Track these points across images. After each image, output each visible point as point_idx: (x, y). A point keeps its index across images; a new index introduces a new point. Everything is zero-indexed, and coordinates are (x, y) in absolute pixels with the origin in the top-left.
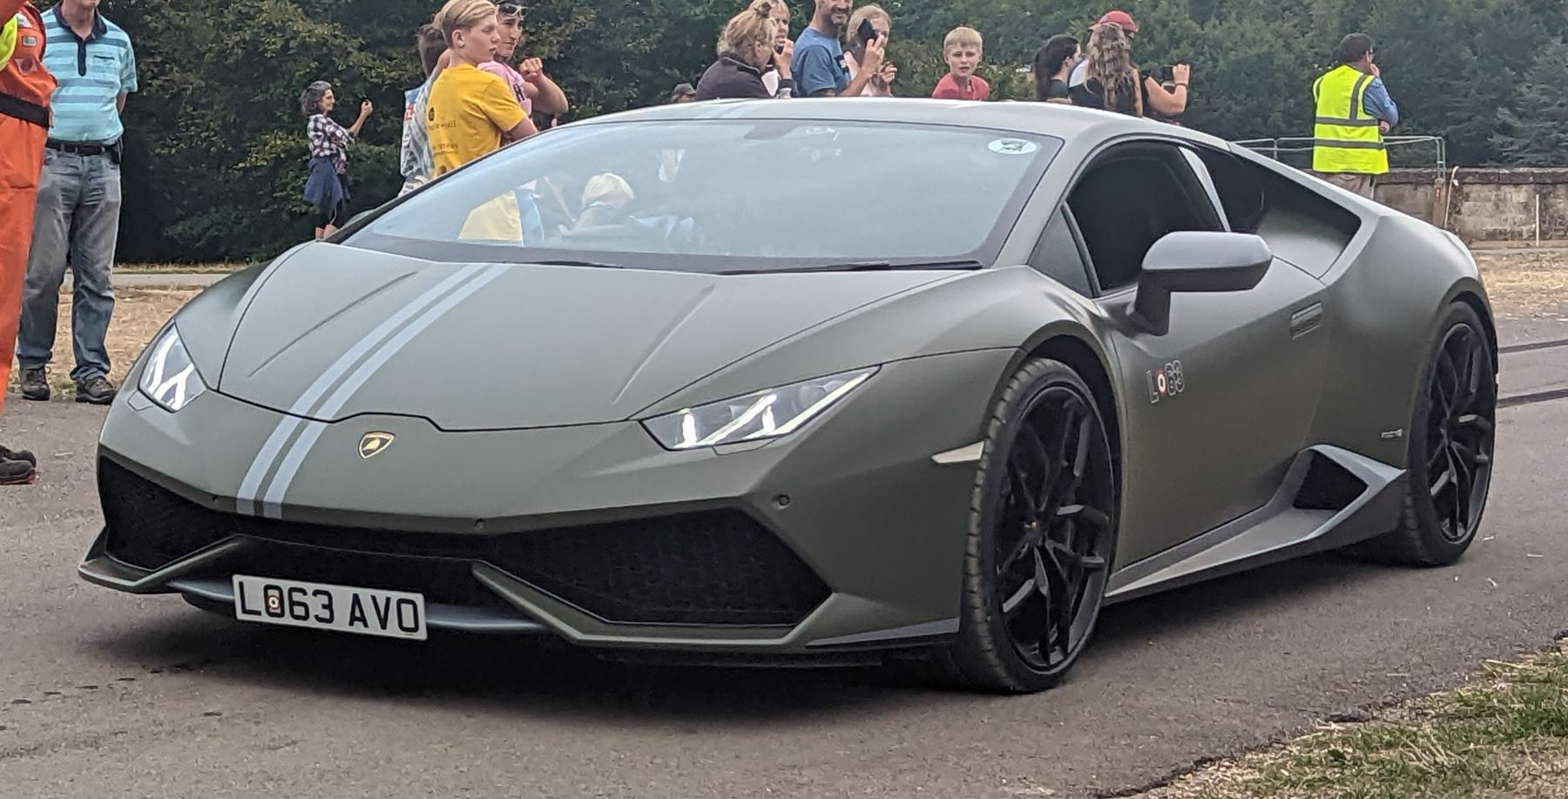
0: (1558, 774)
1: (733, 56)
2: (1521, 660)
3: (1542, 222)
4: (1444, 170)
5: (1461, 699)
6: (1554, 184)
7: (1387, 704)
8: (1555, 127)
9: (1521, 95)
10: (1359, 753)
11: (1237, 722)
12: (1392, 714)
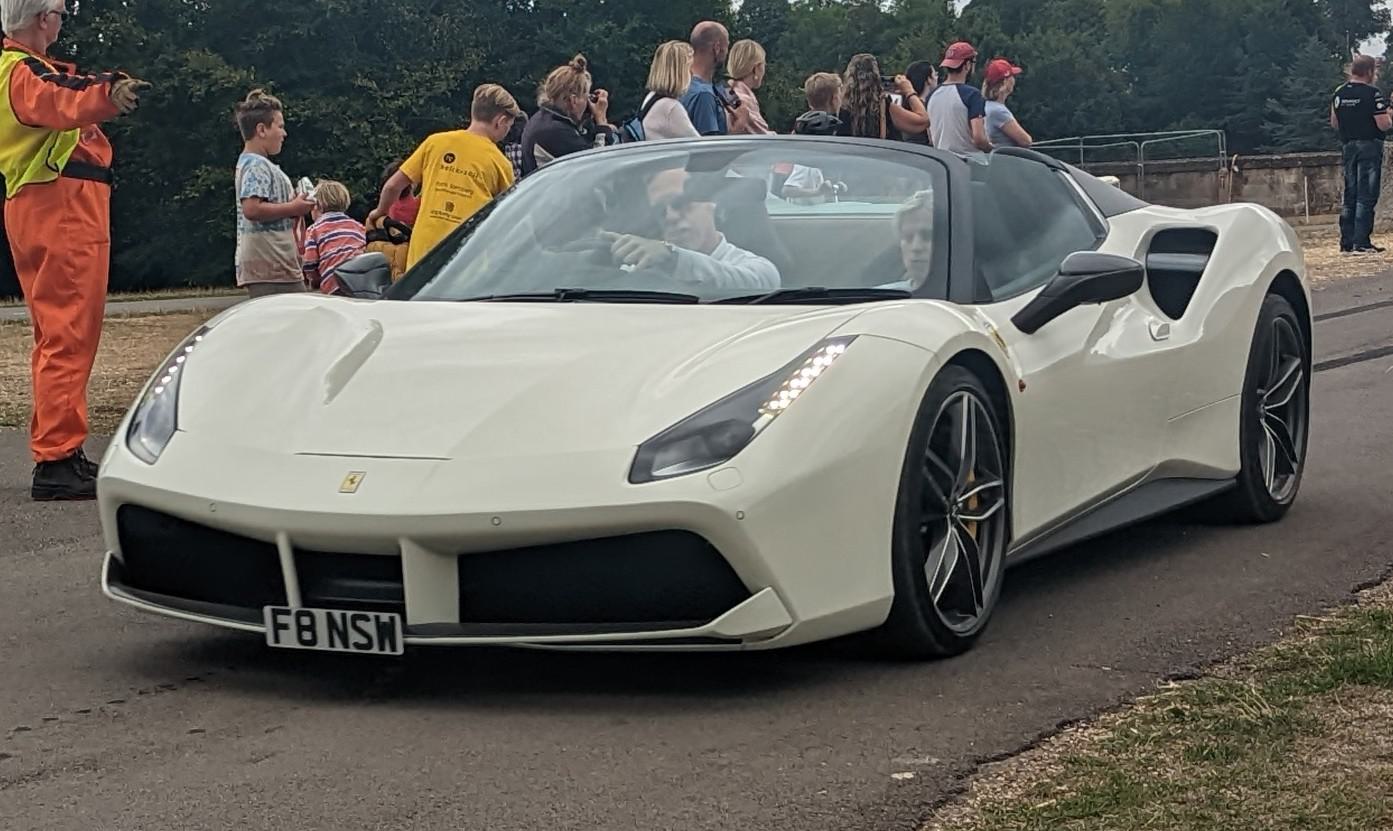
0: (1366, 720)
1: (549, 107)
2: (1326, 614)
3: (1311, 199)
4: (1226, 158)
5: (1278, 653)
6: (1319, 166)
7: (1215, 662)
8: (1316, 113)
9: (1286, 87)
10: (1195, 709)
11: (1089, 686)
12: (1221, 670)
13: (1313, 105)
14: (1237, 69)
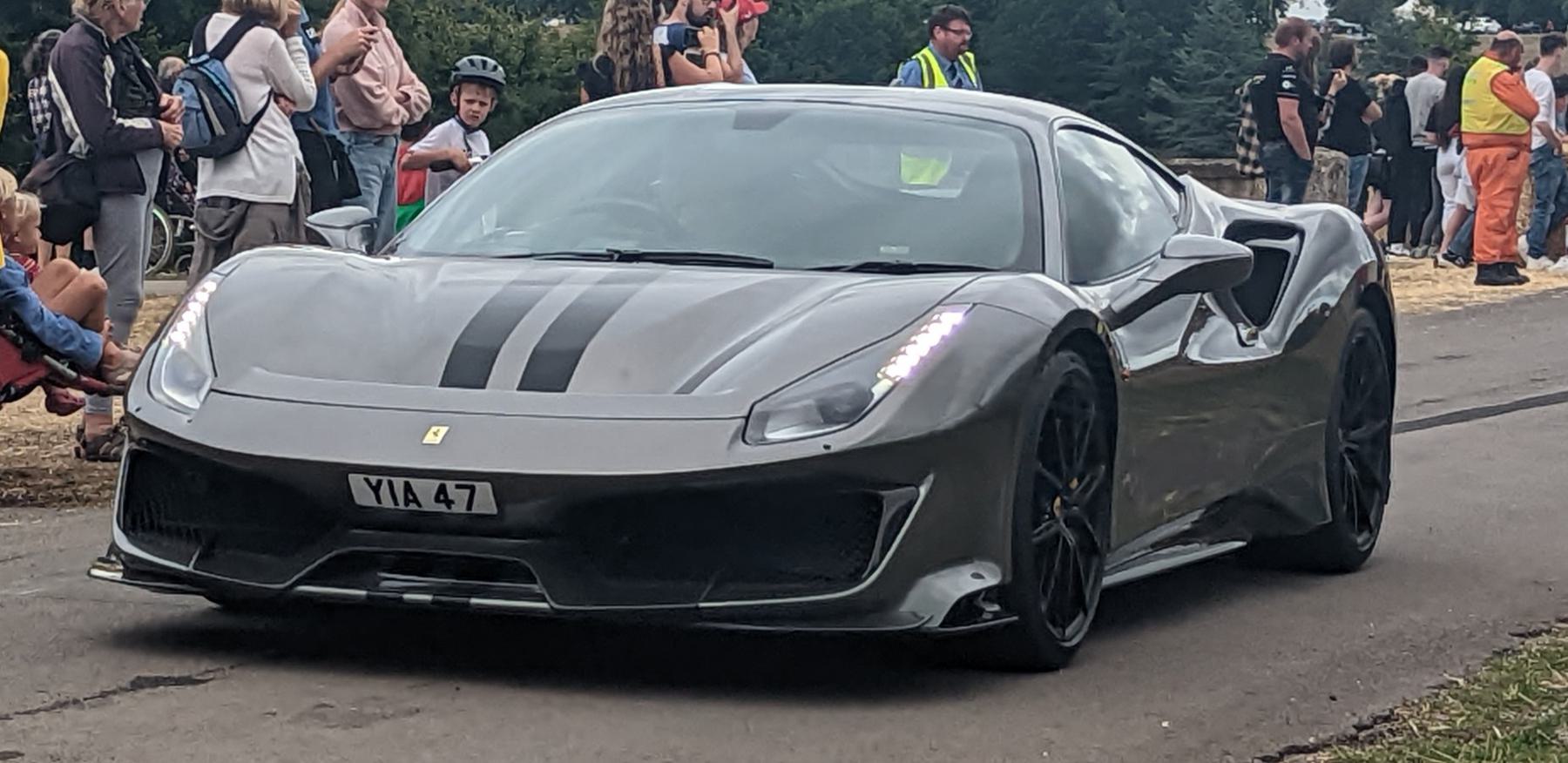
8: (1219, 103)
9: (1180, 62)
13: (1219, 90)
14: (1110, 34)
